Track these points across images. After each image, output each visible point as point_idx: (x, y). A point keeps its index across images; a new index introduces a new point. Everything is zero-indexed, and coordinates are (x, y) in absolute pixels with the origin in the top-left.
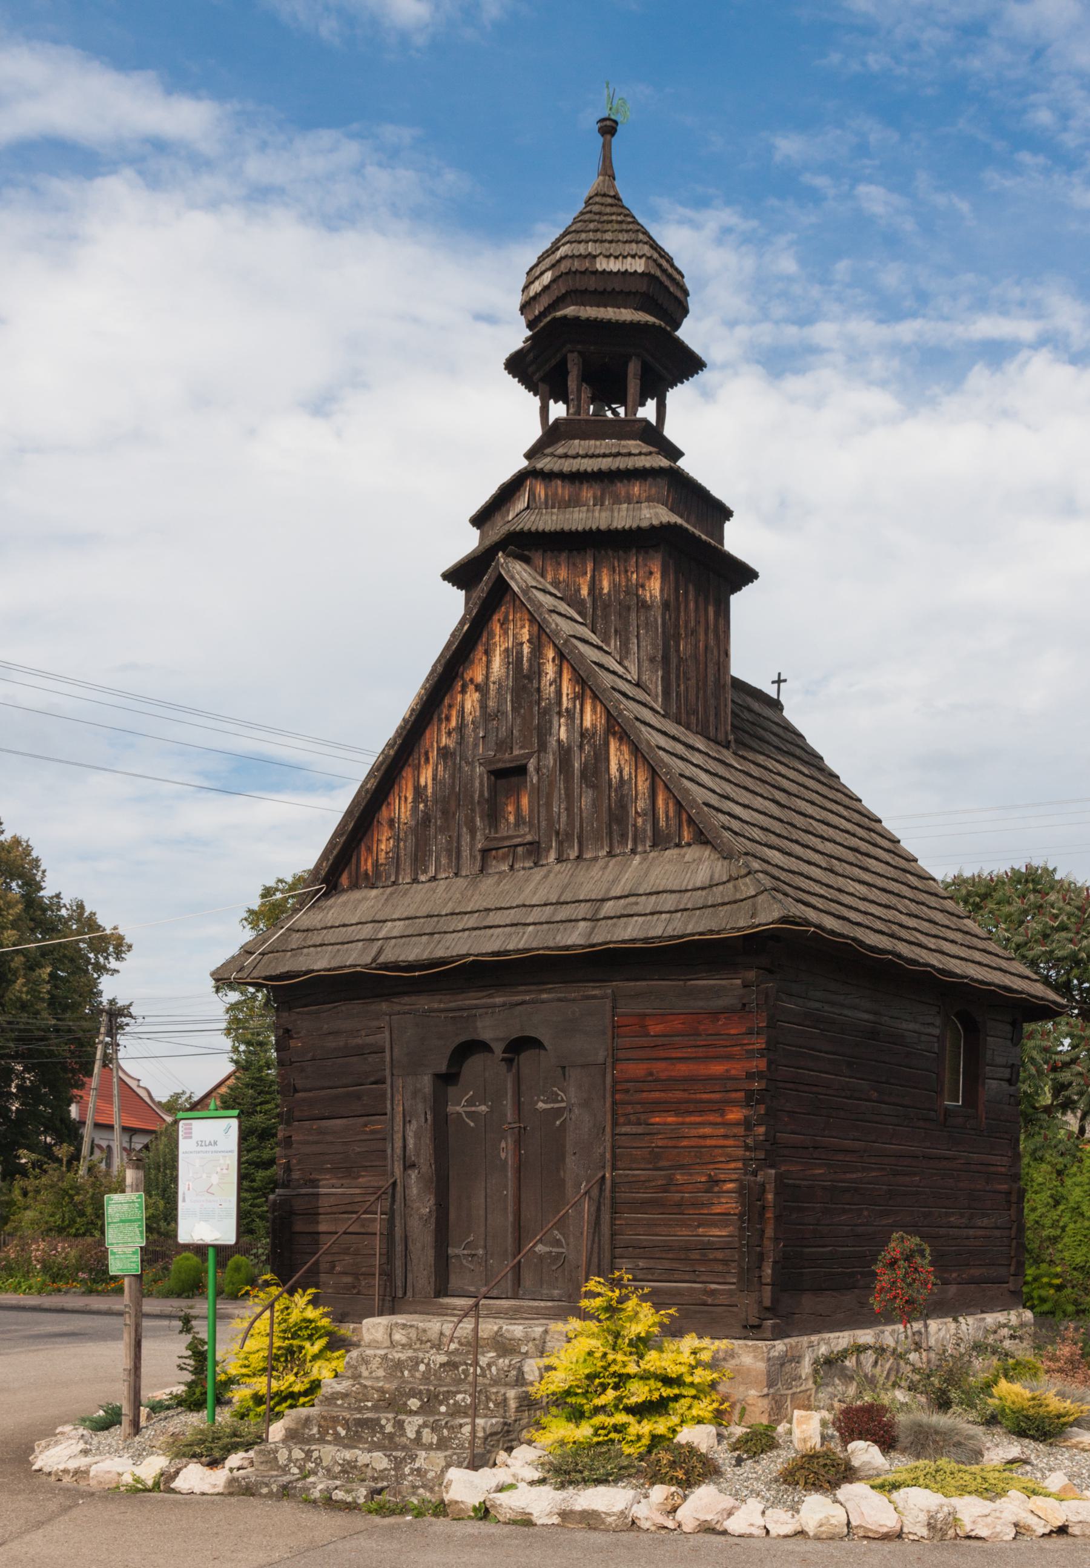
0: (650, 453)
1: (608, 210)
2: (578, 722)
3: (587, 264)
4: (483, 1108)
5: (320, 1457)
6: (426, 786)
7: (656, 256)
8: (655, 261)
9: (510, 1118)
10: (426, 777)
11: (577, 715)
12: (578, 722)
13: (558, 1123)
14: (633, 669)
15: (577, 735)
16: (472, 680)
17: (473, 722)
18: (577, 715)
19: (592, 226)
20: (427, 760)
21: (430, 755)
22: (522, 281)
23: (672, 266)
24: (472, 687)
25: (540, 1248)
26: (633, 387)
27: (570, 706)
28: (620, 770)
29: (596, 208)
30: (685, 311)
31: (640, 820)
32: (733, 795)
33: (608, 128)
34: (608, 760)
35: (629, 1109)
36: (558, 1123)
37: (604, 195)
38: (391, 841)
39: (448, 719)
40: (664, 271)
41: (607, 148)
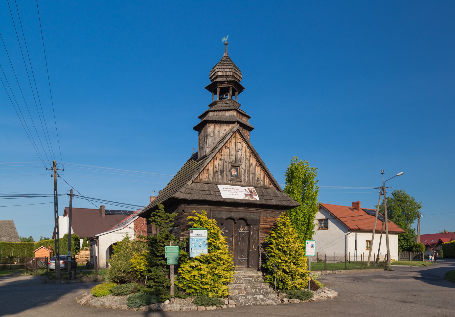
4: (227, 231)
5: (248, 297)
6: (216, 165)
9: (234, 233)
10: (216, 163)
13: (243, 235)
16: (227, 146)
17: (227, 155)
20: (216, 159)
21: (217, 159)
24: (227, 148)
25: (239, 258)
27: (249, 158)
35: (262, 233)
36: (243, 235)
38: (208, 174)
39: (221, 152)
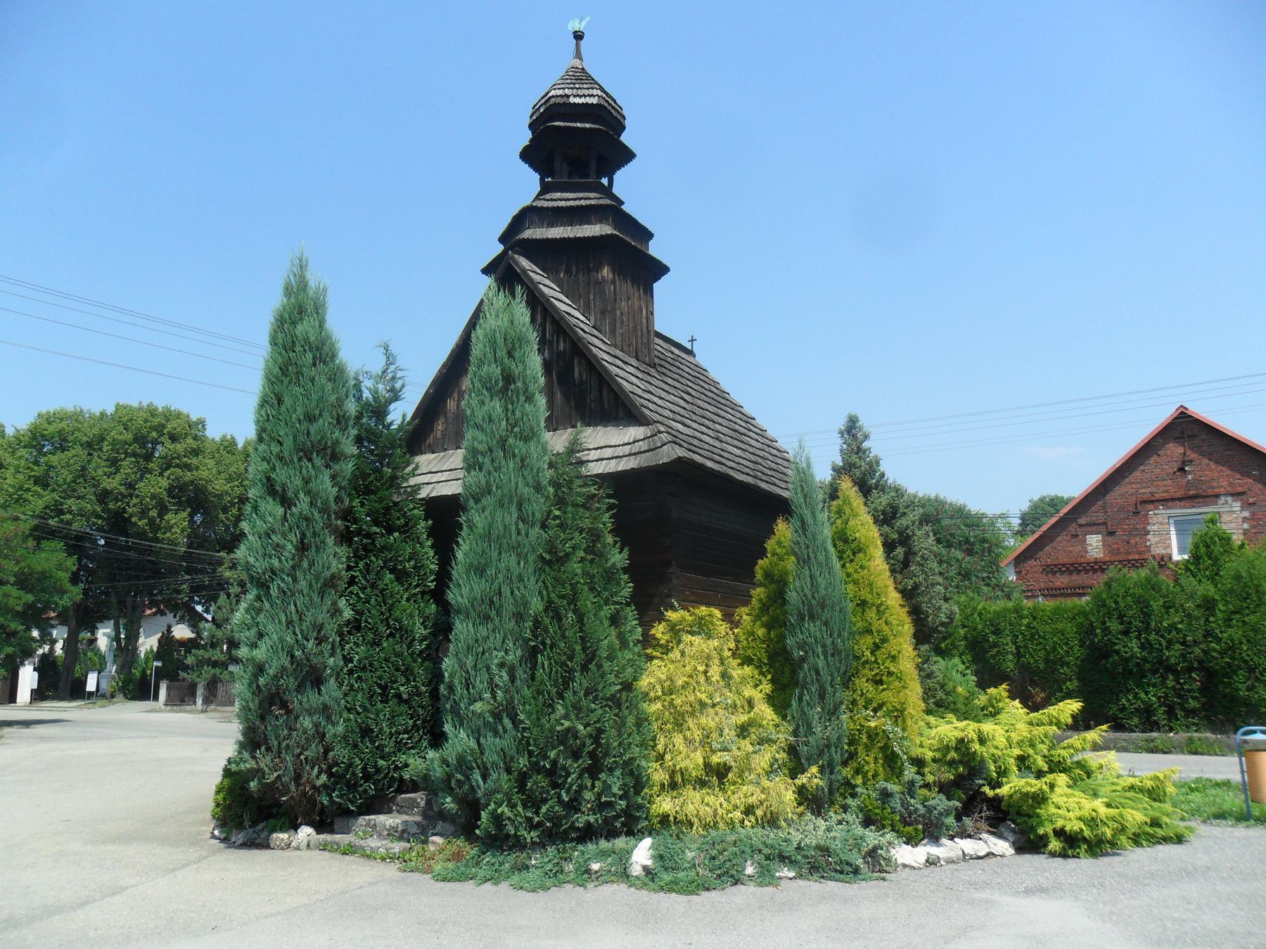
0: (601, 198)
1: (578, 74)
2: (555, 347)
3: (565, 99)
7: (604, 96)
8: (604, 98)
11: (555, 344)
12: (555, 347)
14: (592, 318)
15: (555, 356)
18: (555, 344)
19: (568, 81)
22: (531, 111)
23: (615, 103)
26: (593, 166)
28: (581, 375)
29: (570, 73)
30: (623, 128)
31: (593, 405)
32: (654, 392)
33: (578, 36)
34: (573, 370)
37: (577, 68)
40: (610, 104)
41: (578, 46)
